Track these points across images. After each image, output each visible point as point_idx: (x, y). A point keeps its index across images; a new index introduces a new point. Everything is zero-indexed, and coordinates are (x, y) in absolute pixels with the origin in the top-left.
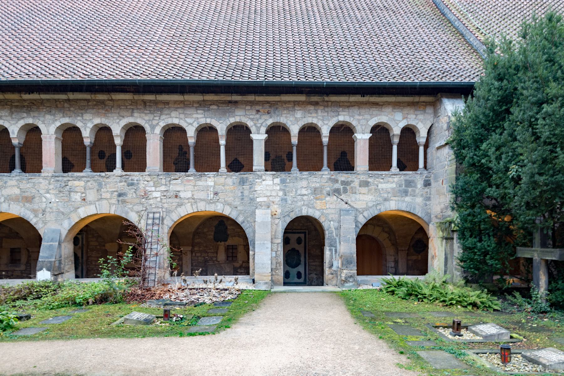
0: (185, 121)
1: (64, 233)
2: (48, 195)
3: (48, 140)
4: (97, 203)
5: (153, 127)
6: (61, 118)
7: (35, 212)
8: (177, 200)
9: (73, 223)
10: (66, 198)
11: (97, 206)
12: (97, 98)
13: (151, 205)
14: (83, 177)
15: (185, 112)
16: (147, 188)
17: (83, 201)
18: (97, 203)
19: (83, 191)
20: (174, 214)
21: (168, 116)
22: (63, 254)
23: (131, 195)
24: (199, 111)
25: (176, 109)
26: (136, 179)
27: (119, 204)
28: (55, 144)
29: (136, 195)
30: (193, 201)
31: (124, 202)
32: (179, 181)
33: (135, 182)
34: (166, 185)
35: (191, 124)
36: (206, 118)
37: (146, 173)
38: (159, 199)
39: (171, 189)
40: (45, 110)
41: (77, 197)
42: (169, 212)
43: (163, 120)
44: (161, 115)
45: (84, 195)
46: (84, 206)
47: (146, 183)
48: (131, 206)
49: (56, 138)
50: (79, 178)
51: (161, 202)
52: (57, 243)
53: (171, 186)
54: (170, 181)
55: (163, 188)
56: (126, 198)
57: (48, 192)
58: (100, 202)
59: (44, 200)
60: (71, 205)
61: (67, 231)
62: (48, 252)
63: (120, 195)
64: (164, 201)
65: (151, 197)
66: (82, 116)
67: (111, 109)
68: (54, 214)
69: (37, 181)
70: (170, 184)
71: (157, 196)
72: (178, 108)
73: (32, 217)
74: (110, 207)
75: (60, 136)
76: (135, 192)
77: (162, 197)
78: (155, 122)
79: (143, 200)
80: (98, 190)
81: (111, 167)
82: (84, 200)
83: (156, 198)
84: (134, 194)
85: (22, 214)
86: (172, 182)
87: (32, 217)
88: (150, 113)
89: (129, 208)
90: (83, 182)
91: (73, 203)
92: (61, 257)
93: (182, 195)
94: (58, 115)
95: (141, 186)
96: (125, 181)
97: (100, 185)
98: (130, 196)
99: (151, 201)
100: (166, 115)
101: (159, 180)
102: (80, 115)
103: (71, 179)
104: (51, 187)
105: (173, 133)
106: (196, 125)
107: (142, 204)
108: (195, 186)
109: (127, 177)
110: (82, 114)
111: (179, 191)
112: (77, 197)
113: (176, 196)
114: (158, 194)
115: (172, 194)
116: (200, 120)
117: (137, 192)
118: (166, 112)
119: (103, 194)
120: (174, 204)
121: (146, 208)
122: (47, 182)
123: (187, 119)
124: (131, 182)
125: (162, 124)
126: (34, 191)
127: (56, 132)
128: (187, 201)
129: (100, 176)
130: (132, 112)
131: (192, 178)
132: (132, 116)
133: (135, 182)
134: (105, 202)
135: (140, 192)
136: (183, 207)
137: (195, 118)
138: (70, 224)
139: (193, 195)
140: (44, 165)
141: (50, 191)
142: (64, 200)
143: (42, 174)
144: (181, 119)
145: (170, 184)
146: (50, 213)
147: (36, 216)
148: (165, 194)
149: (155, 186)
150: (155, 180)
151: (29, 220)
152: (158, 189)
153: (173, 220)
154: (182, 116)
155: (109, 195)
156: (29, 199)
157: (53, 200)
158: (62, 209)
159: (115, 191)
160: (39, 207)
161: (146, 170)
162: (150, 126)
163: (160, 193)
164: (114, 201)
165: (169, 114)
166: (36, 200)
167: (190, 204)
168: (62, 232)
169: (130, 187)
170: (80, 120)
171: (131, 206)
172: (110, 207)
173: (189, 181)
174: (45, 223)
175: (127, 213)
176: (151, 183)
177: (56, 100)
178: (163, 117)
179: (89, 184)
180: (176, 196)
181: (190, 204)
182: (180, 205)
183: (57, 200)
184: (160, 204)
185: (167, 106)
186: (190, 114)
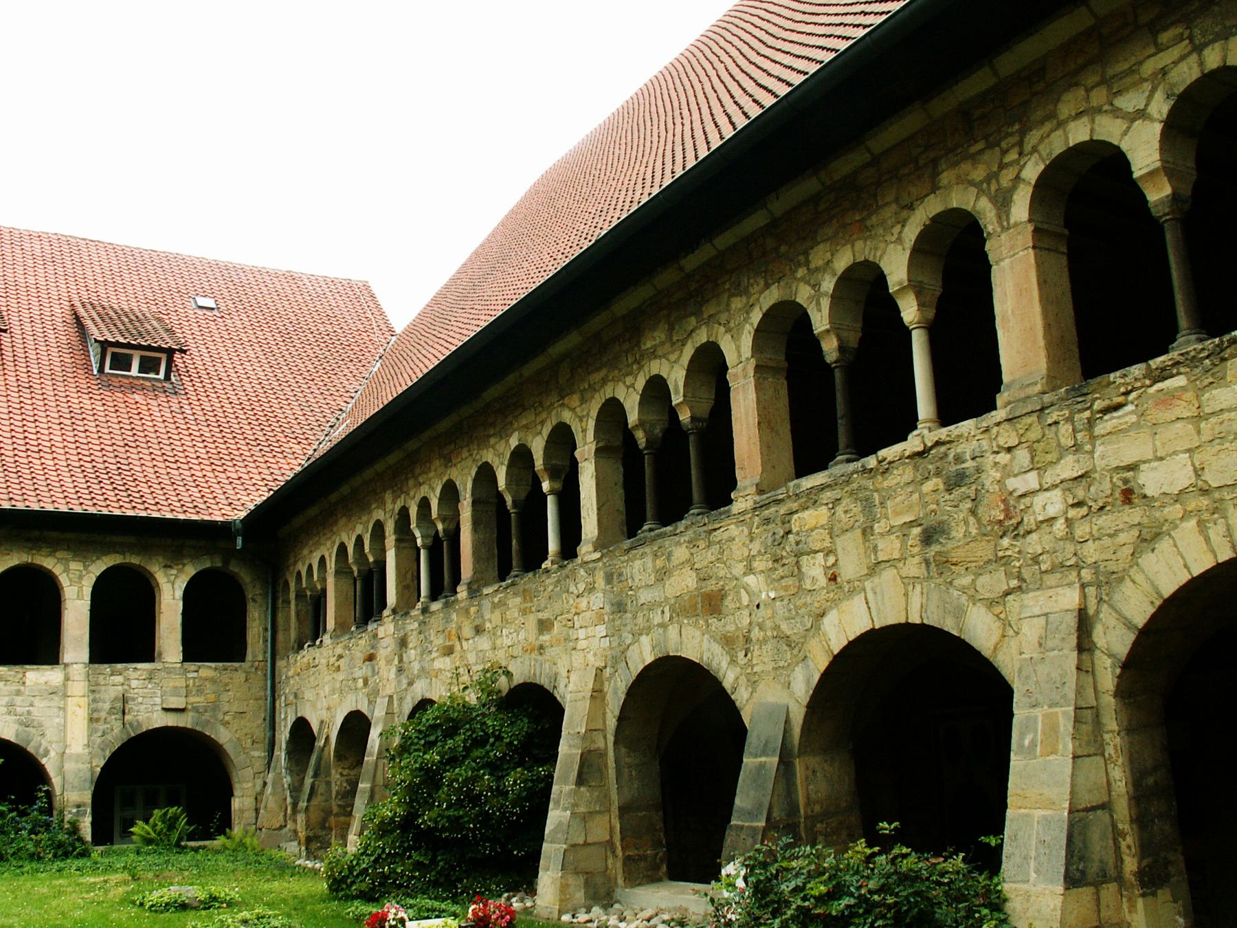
0: (1116, 113)
1: (798, 716)
2: (751, 580)
3: (742, 381)
4: (868, 585)
5: (1003, 202)
6: (761, 292)
7: (727, 642)
8: (1135, 515)
9: (817, 677)
10: (790, 581)
11: (870, 596)
12: (837, 177)
13: (1035, 560)
14: (823, 488)
15: (1110, 72)
16: (1012, 483)
17: (833, 586)
18: (868, 585)
19: (827, 544)
20: (1127, 588)
21: (1048, 126)
22: (802, 801)
23: (962, 530)
24: (1164, 37)
25: (1071, 81)
26: (966, 449)
27: (930, 578)
28: (758, 388)
29: (979, 521)
30: (1204, 502)
31: (943, 564)
32: (1127, 415)
33: (970, 464)
34: (1077, 448)
35: (1142, 114)
36: (1198, 49)
37: (999, 414)
38: (1060, 525)
39: (1100, 464)
40: (727, 286)
41: (814, 569)
42: (1107, 580)
43: (1035, 149)
44: (1023, 133)
45: (831, 559)
46: (835, 603)
47: (1003, 458)
48: (966, 580)
49: (758, 368)
50: (811, 499)
51: (1070, 536)
52: (776, 759)
53: (1099, 450)
54: (1091, 423)
55: (1068, 468)
56: (950, 545)
57: (750, 570)
58: (876, 580)
59: (745, 600)
60: (805, 604)
61: (803, 711)
62: (752, 793)
63: (928, 538)
64: (1081, 530)
65: (1029, 521)
66: (807, 263)
67: (875, 196)
68: (769, 646)
69: (726, 535)
70: (1093, 438)
71: (1052, 511)
72: (1076, 72)
73: (724, 664)
74: (906, 594)
75: (778, 358)
76: (973, 512)
77: (1072, 513)
78: (1006, 178)
79: (1006, 542)
80: (864, 532)
81: (901, 423)
82: (833, 578)
83: (1051, 520)
84: (972, 520)
85: (705, 658)
86: (1099, 429)
87: (724, 664)
88: (990, 146)
89: (963, 590)
90: (823, 509)
91: (809, 600)
92: (793, 809)
93: (1151, 481)
94: (756, 288)
95: (991, 476)
96: (938, 473)
97: (868, 505)
98: (958, 532)
99: (1034, 544)
100: (1042, 123)
101: (1050, 433)
102: (802, 258)
103: (795, 506)
104: (756, 547)
105: (1088, 193)
106: (1160, 107)
107: (1004, 561)
108: (1199, 417)
109: (943, 449)
110: (806, 253)
111: (1133, 467)
112: (814, 569)
113: (1128, 496)
114: (1053, 503)
115: (1107, 486)
116: (1174, 76)
117: (980, 510)
118: (1040, 114)
119: (881, 545)
120: (1122, 538)
121: (1020, 578)
122: (746, 531)
123: (1120, 102)
124: (953, 468)
125: (1032, 171)
126: (722, 573)
127: (757, 347)
128: (1174, 511)
129: (865, 470)
130: (935, 174)
131: (1179, 381)
132: (934, 189)
133: (970, 464)
134: (888, 574)
135: (990, 507)
136: (1164, 545)
137: (1155, 74)
138: (808, 681)
139: (1198, 472)
140: (739, 474)
141: (755, 564)
142: (786, 588)
143: (736, 507)
144: (1099, 110)
145: (1093, 438)
146: (764, 641)
147: (733, 661)
148: (1081, 494)
149: (1037, 467)
150: (1034, 434)
151: (720, 676)
152: (1049, 478)
153: (1128, 624)
154: (1099, 96)
155: (897, 544)
156: (711, 603)
157: (764, 596)
158: (784, 626)
159: (911, 524)
160: (738, 628)
161: (1000, 399)
162: (993, 200)
163: (1057, 493)
164: (913, 567)
165: (1052, 116)
166: (729, 603)
167: (1192, 523)
168: (791, 715)
169: (957, 493)
170: (802, 279)
171: (966, 580)
172: (906, 594)
173: (1169, 398)
174: (753, 684)
175: (959, 613)
176: (1023, 456)
177: (748, 240)
178: (1033, 138)
179: (840, 510)
180: (1128, 496)
181: (1192, 523)
182: (1149, 538)
183: (772, 595)
184: (1070, 548)
185: (1039, 87)
186: (1131, 71)
